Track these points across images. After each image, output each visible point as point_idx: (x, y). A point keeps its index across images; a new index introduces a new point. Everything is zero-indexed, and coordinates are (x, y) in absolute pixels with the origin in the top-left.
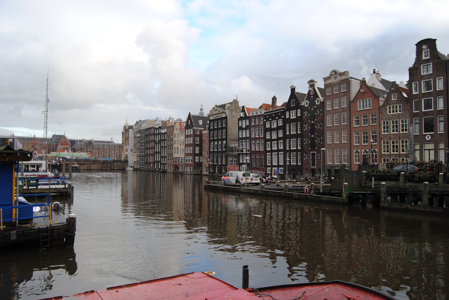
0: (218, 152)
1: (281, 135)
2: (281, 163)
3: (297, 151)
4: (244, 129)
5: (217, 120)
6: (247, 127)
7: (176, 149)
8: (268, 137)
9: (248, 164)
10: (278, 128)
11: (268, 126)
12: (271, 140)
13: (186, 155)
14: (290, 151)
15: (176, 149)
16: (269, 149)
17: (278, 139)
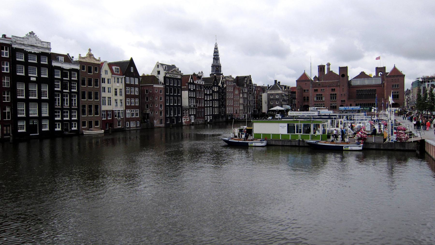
0: (174, 106)
1: (211, 99)
2: (211, 114)
3: (217, 107)
4: (192, 91)
5: (173, 79)
6: (194, 90)
7: (107, 99)
8: (206, 99)
9: (195, 115)
10: (210, 95)
11: (206, 93)
12: (207, 101)
13: (127, 107)
14: (215, 107)
15: (107, 99)
16: (206, 106)
17: (210, 100)
